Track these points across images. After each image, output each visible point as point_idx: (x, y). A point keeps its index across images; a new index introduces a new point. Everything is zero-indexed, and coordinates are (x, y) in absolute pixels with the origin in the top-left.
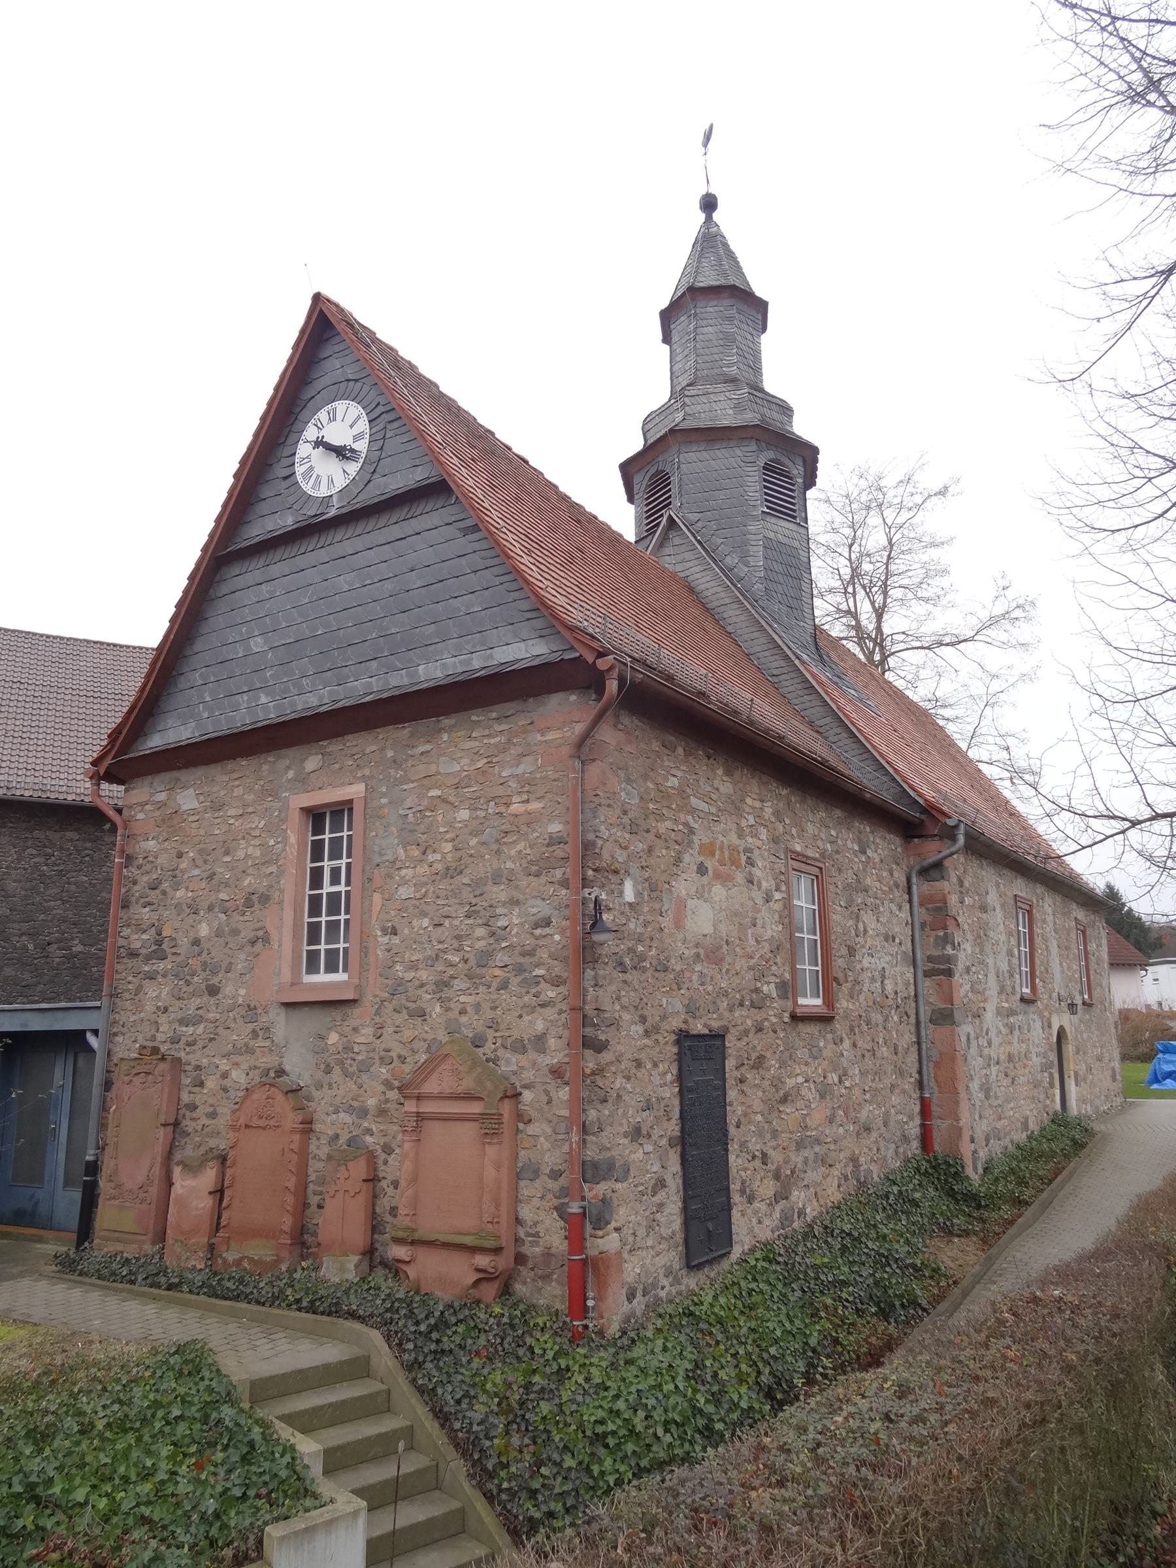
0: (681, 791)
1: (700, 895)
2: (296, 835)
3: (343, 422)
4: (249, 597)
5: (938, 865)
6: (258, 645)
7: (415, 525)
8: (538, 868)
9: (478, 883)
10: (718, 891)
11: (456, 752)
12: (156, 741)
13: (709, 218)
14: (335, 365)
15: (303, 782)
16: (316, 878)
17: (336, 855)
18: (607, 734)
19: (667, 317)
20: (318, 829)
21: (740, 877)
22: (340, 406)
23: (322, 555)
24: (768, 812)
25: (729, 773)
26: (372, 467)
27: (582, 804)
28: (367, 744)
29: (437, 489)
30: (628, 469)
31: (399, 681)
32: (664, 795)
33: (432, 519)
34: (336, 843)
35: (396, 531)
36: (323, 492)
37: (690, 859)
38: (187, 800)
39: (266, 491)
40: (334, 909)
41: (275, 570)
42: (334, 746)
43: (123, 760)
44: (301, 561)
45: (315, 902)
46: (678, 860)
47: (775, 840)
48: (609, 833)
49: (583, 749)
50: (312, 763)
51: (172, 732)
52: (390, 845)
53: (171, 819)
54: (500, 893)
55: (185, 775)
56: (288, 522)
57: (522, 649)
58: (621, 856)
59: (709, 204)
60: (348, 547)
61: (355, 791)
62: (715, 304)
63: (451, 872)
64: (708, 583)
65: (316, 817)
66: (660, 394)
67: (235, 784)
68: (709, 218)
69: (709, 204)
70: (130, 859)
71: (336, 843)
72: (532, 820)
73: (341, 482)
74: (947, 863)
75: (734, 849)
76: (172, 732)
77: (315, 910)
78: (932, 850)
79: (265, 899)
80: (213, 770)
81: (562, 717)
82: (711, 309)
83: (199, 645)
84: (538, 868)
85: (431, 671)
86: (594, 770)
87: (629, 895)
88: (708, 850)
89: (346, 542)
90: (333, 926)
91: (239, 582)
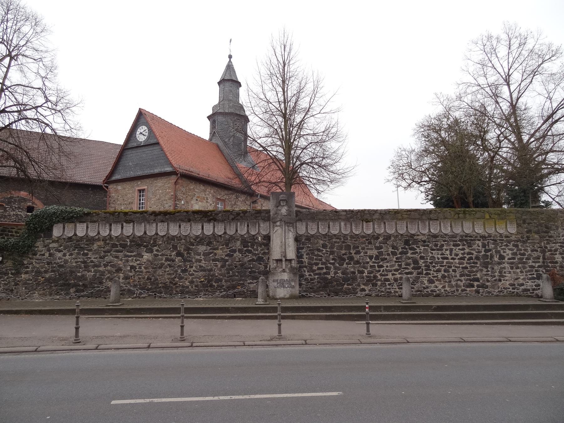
0: (193, 189)
1: (196, 203)
2: (137, 193)
3: (143, 129)
4: (129, 156)
5: (255, 201)
6: (130, 164)
7: (155, 148)
8: (170, 199)
9: (162, 201)
10: (200, 203)
11: (160, 183)
12: (114, 178)
13: (230, 60)
14: (142, 120)
15: (138, 186)
16: (140, 200)
17: (143, 197)
18: (180, 181)
19: (219, 83)
20: (140, 193)
21: (205, 201)
22: (144, 127)
23: (141, 151)
24: (212, 191)
25: (204, 186)
26: (149, 138)
27: (175, 191)
28: (148, 180)
29: (158, 144)
30: (209, 117)
31: (152, 172)
32: (190, 189)
33: (156, 147)
34: (143, 195)
35: (152, 149)
36: (141, 140)
37: (195, 198)
38: (119, 188)
39: (132, 139)
40: (142, 204)
41: (133, 152)
42: (142, 181)
43: (109, 180)
44: (138, 151)
45: (140, 203)
46: (192, 199)
47: (213, 196)
48: (180, 195)
49: (176, 183)
50: (139, 183)
51: (116, 177)
52: (150, 195)
53: (117, 191)
54: (165, 202)
55: (119, 184)
56: (135, 144)
57: (169, 169)
58: (181, 198)
59: (230, 57)
60: (145, 150)
61: (146, 187)
62: (230, 82)
63: (158, 199)
64: (221, 144)
65: (140, 191)
66: (216, 101)
67: (127, 186)
68: (230, 60)
69: (230, 57)
70: (110, 197)
71: (143, 195)
72: (169, 192)
73: (144, 140)
74: (258, 201)
75: (203, 197)
76: (116, 177)
77: (140, 205)
78: (255, 199)
79: (132, 203)
80: (124, 183)
81: (173, 178)
82: (227, 84)
83: (121, 163)
84: (170, 199)
85: (157, 171)
86: (177, 186)
87: (183, 202)
88: (198, 197)
89: (144, 149)
90: (142, 207)
91: (127, 153)
